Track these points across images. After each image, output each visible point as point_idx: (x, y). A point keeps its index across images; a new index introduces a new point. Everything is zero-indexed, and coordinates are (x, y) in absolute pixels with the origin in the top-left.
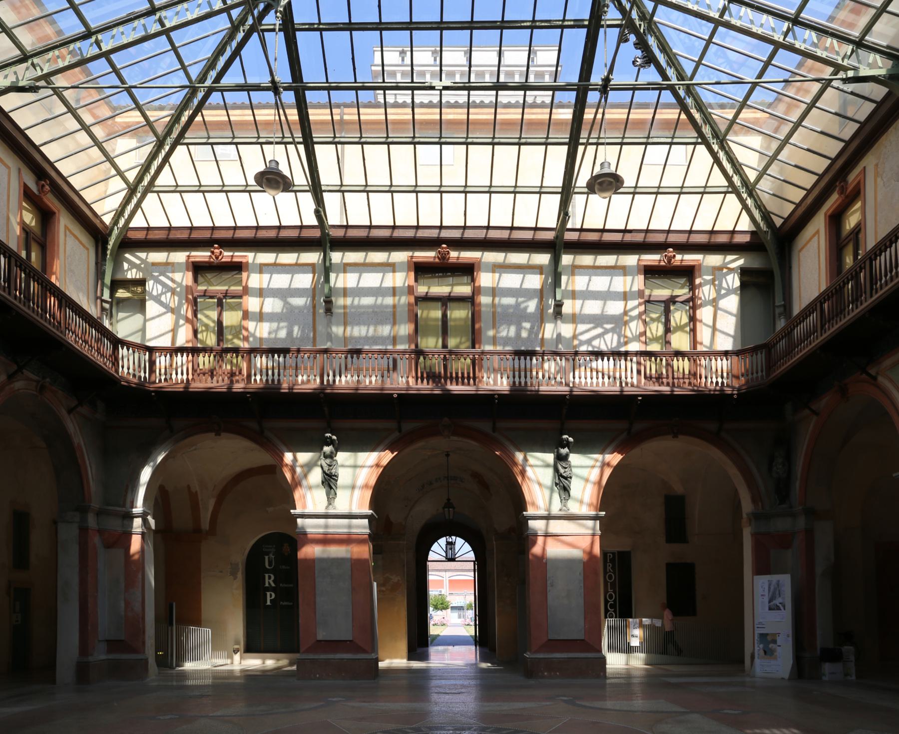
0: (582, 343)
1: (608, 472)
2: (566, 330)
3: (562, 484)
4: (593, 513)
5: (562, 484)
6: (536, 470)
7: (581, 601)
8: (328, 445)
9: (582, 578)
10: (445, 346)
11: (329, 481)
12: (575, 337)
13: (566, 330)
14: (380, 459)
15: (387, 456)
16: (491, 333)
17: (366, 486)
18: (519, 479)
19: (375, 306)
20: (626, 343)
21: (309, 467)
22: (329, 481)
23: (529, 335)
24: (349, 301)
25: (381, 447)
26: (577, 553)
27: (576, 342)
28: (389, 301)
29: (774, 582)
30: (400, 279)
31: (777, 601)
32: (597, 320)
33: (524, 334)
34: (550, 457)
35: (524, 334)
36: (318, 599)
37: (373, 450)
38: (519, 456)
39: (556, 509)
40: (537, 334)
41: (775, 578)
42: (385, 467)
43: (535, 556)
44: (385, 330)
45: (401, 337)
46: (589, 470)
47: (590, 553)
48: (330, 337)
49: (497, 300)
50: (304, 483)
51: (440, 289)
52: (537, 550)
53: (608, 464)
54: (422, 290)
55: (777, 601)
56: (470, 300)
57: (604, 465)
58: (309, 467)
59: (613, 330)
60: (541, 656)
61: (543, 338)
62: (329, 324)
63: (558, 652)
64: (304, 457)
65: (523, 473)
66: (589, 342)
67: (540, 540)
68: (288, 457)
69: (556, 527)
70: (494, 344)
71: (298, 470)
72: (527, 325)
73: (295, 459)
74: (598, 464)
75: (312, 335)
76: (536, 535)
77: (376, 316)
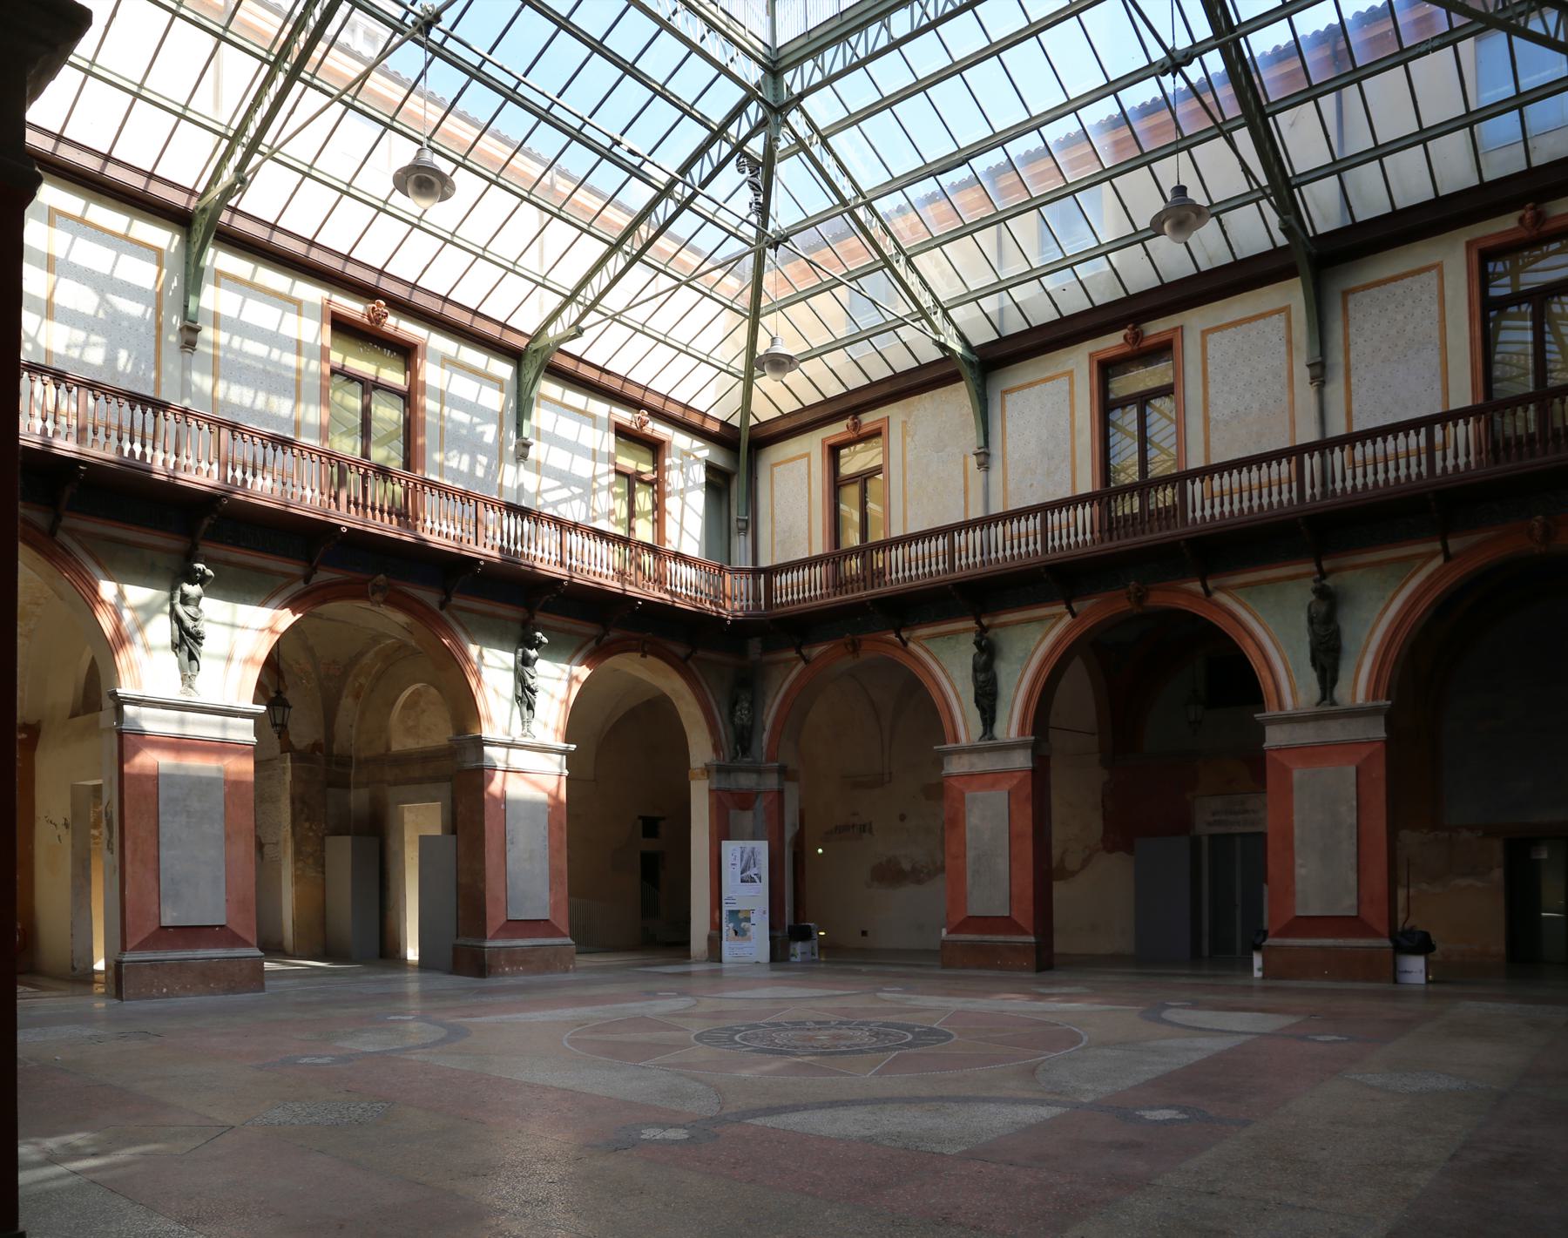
0: (546, 504)
1: (576, 688)
2: (530, 480)
3: (525, 696)
4: (562, 745)
5: (525, 696)
6: (492, 669)
7: (547, 866)
8: (193, 583)
9: (546, 833)
10: (365, 455)
11: (187, 641)
12: (538, 493)
13: (530, 480)
14: (275, 620)
15: (286, 619)
16: (438, 457)
17: (249, 660)
18: (473, 682)
19: (266, 360)
20: (594, 519)
21: (148, 611)
22: (187, 641)
23: (487, 473)
24: (223, 337)
25: (276, 601)
26: (542, 796)
27: (540, 501)
28: (290, 359)
29: (748, 850)
30: (314, 332)
31: (751, 872)
32: (566, 479)
33: (480, 472)
34: (509, 658)
35: (480, 472)
36: (164, 854)
37: (263, 604)
38: (473, 650)
39: (517, 734)
40: (494, 478)
41: (749, 844)
42: (284, 635)
43: (493, 797)
44: (283, 406)
45: (309, 425)
46: (559, 680)
47: (555, 797)
48: (185, 387)
49: (446, 410)
50: (138, 638)
51: (363, 366)
52: (495, 787)
53: (576, 678)
54: (336, 358)
55: (751, 872)
56: (408, 398)
57: (572, 679)
58: (148, 611)
59: (580, 496)
60: (500, 943)
61: (501, 485)
62: (186, 368)
63: (522, 937)
64: (138, 594)
65: (478, 674)
66: (555, 505)
67: (499, 775)
68: (107, 589)
69: (518, 758)
70: (441, 475)
71: (127, 615)
72: (483, 459)
73: (121, 595)
74: (566, 676)
75: (153, 375)
76: (494, 769)
77: (267, 378)
